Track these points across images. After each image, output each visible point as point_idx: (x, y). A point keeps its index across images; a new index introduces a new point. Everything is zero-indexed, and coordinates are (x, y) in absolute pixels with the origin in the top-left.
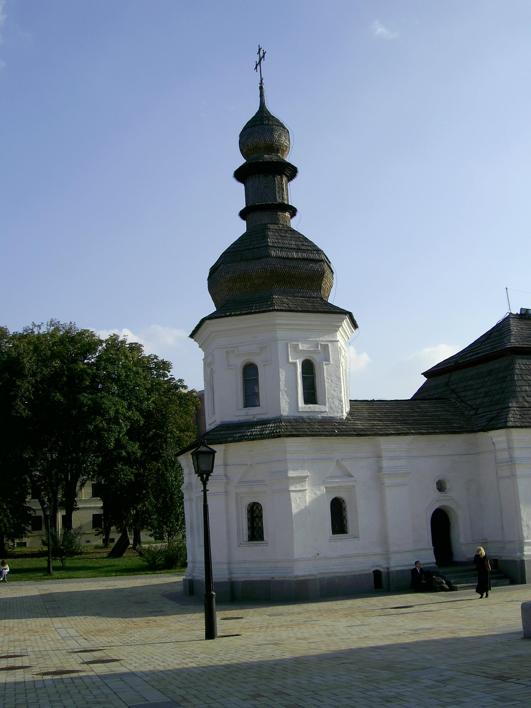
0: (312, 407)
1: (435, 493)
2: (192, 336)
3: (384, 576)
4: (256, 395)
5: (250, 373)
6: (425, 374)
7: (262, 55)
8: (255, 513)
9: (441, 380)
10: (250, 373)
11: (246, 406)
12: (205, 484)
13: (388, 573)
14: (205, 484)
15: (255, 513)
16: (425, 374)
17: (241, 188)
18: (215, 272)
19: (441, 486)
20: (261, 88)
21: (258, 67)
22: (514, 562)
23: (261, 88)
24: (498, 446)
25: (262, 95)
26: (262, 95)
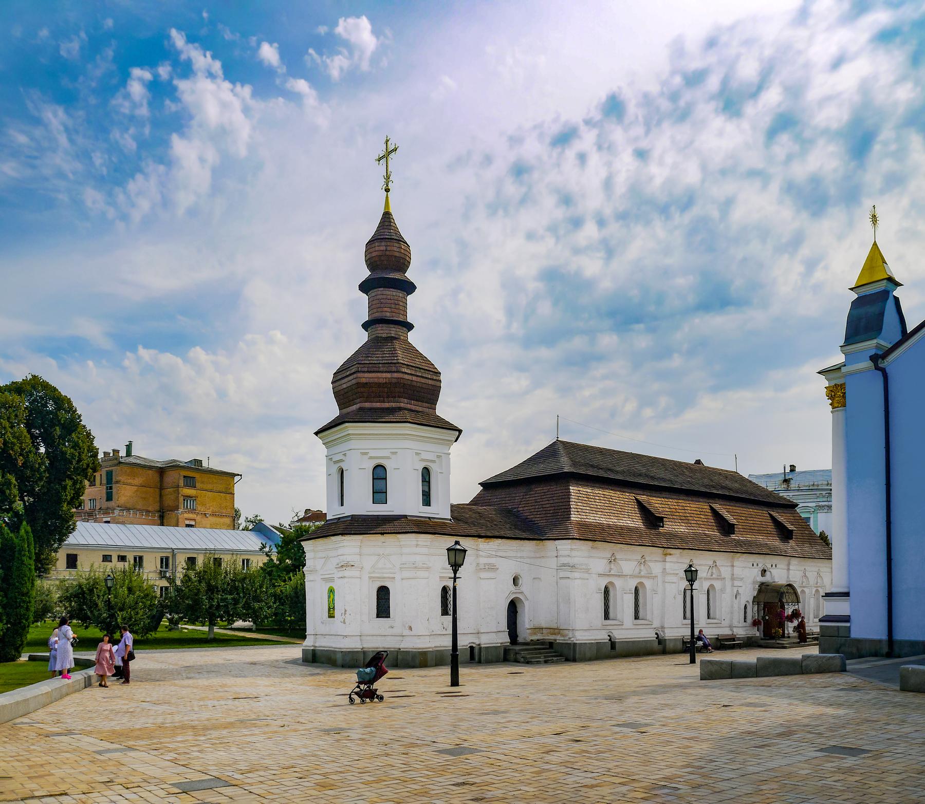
0: (427, 509)
3: (476, 651)
5: (379, 474)
8: (383, 594)
10: (379, 474)
13: (480, 648)
15: (383, 594)
19: (515, 581)
24: (561, 553)
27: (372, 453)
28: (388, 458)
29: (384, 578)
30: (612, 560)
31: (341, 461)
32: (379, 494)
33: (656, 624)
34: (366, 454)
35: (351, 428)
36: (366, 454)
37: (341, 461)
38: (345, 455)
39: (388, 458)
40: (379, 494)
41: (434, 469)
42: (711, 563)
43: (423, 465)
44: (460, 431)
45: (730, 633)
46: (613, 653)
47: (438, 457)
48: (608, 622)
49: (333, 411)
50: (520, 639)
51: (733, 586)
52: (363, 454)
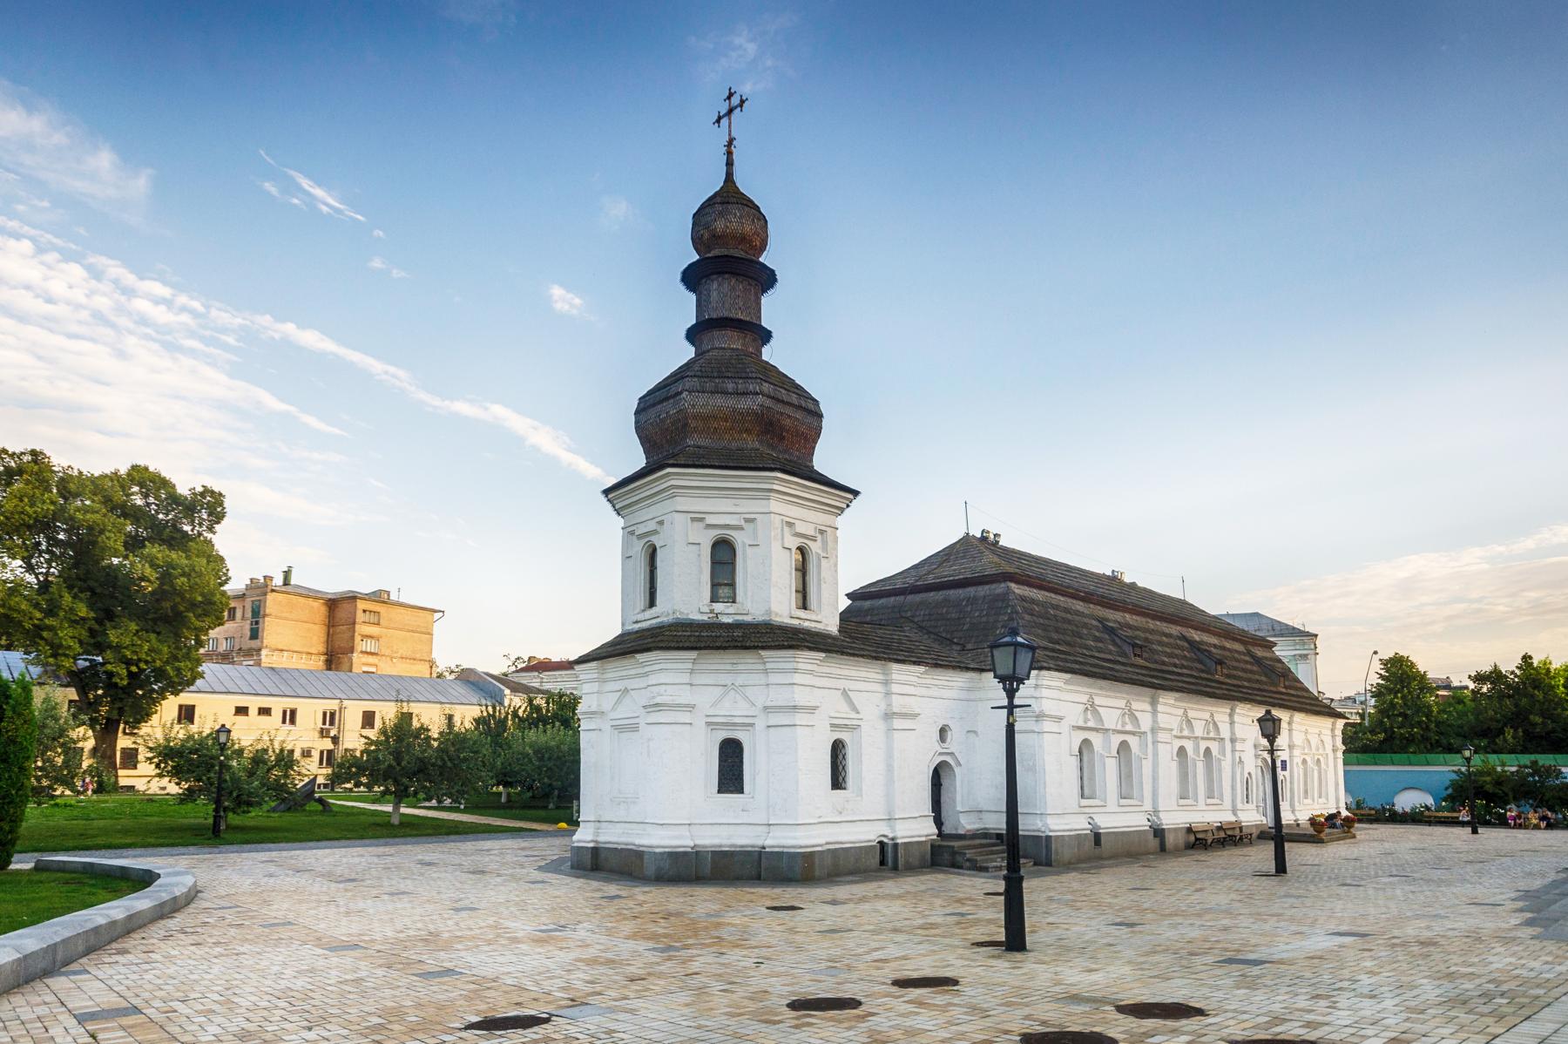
0: (801, 614)
1: (938, 748)
4: (732, 585)
5: (723, 555)
6: (849, 596)
9: (858, 603)
10: (723, 555)
11: (712, 601)
16: (849, 596)
18: (646, 405)
27: (711, 520)
28: (739, 528)
29: (734, 724)
30: (1091, 708)
31: (655, 532)
33: (1148, 806)
34: (702, 520)
35: (675, 477)
36: (702, 520)
37: (655, 532)
38: (661, 523)
39: (739, 528)
41: (815, 548)
42: (1207, 716)
43: (798, 542)
44: (856, 493)
45: (1233, 819)
47: (822, 532)
49: (638, 460)
51: (1233, 751)
52: (693, 520)
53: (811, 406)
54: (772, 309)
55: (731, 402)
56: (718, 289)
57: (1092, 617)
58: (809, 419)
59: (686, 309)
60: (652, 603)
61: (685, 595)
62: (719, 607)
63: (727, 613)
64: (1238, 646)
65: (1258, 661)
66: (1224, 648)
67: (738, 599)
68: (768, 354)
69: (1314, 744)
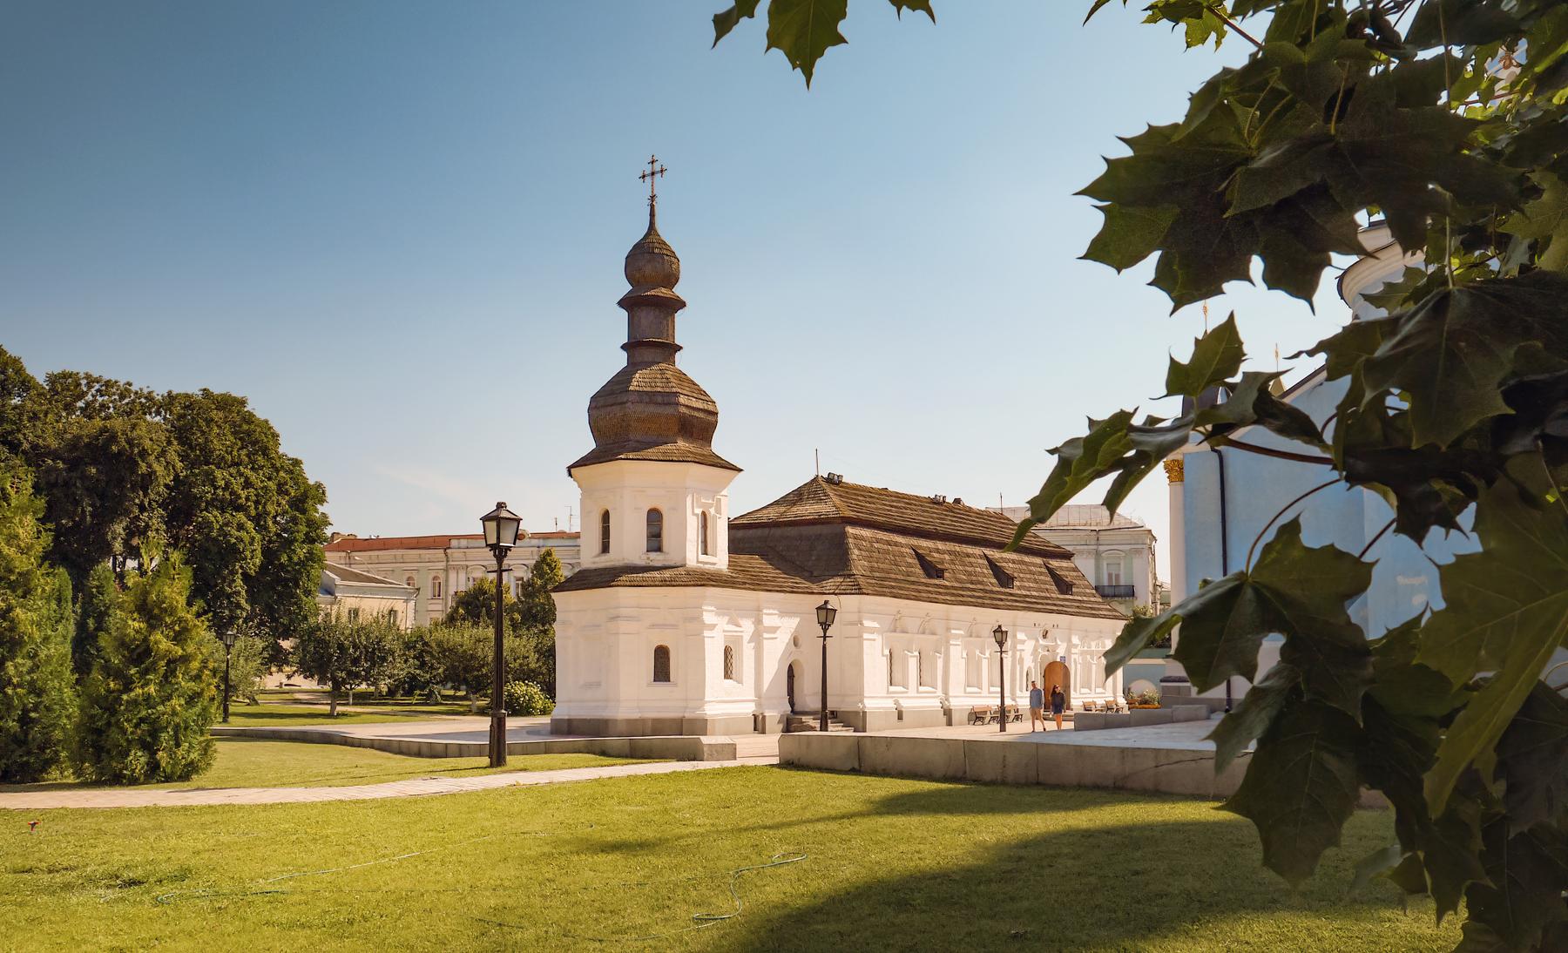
0: (703, 558)
2: (569, 469)
5: (655, 517)
7: (657, 167)
8: (662, 656)
10: (655, 517)
12: (825, 631)
14: (825, 631)
15: (662, 655)
17: (624, 314)
20: (652, 207)
21: (648, 179)
22: (857, 713)
23: (652, 207)
25: (652, 215)
26: (652, 215)
32: (655, 539)
40: (655, 539)
46: (900, 723)
48: (892, 689)
49: (588, 444)
50: (797, 708)
53: (711, 408)
54: (684, 327)
55: (660, 410)
56: (647, 317)
57: (907, 546)
58: (710, 418)
59: (618, 326)
60: (605, 548)
61: (630, 545)
62: (653, 555)
63: (656, 559)
64: (1038, 560)
65: (1051, 572)
66: (1023, 562)
67: (665, 548)
68: (682, 361)
69: (1084, 644)
